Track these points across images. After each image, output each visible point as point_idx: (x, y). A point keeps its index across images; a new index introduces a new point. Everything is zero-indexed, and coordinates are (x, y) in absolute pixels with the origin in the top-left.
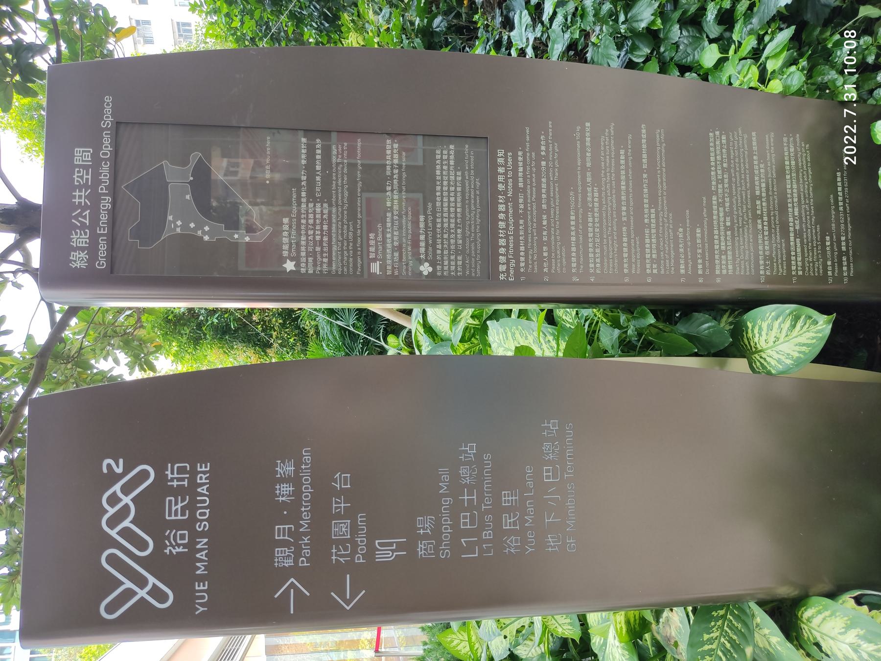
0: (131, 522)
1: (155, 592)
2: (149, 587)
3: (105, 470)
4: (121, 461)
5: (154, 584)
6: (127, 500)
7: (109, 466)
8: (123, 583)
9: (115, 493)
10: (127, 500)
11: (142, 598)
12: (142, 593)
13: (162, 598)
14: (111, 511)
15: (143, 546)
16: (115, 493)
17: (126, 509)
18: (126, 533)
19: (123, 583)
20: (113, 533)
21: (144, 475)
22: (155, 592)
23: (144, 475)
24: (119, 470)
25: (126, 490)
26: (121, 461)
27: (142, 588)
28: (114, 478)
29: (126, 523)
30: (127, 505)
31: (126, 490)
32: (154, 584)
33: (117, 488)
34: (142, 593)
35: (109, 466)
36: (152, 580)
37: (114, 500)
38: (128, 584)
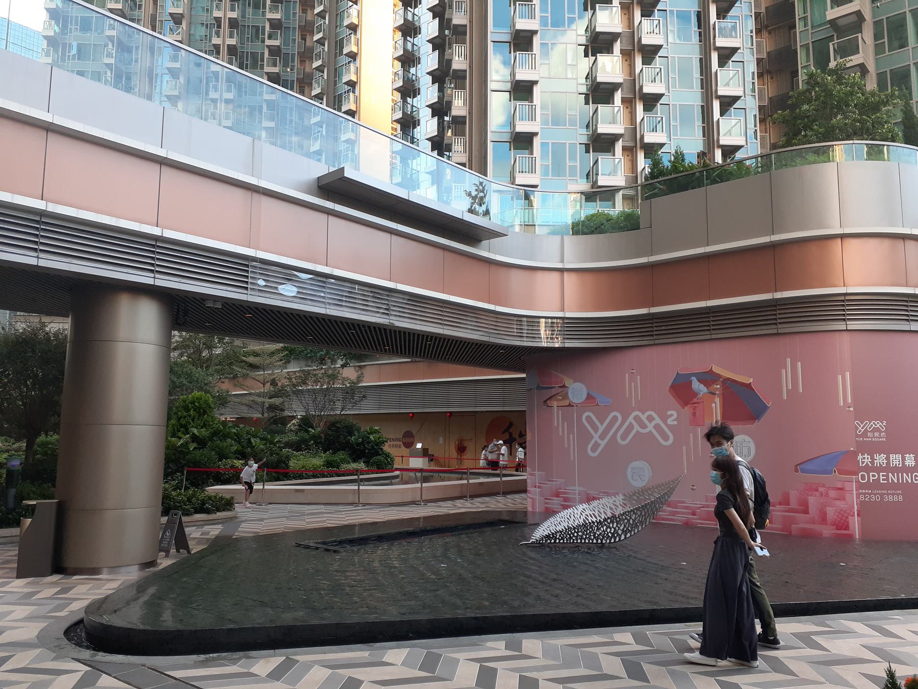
1: (596, 445)
2: (599, 441)
3: (669, 413)
4: (676, 423)
6: (650, 427)
7: (672, 415)
8: (602, 424)
10: (650, 427)
13: (594, 449)
14: (644, 417)
15: (623, 438)
17: (645, 427)
18: (631, 427)
19: (602, 424)
21: (666, 438)
22: (596, 445)
23: (666, 438)
25: (657, 427)
26: (676, 423)
27: (600, 437)
28: (664, 419)
29: (637, 428)
31: (657, 427)
33: (658, 420)
34: (596, 437)
35: (672, 415)
36: (603, 443)
37: (650, 419)
38: (601, 429)
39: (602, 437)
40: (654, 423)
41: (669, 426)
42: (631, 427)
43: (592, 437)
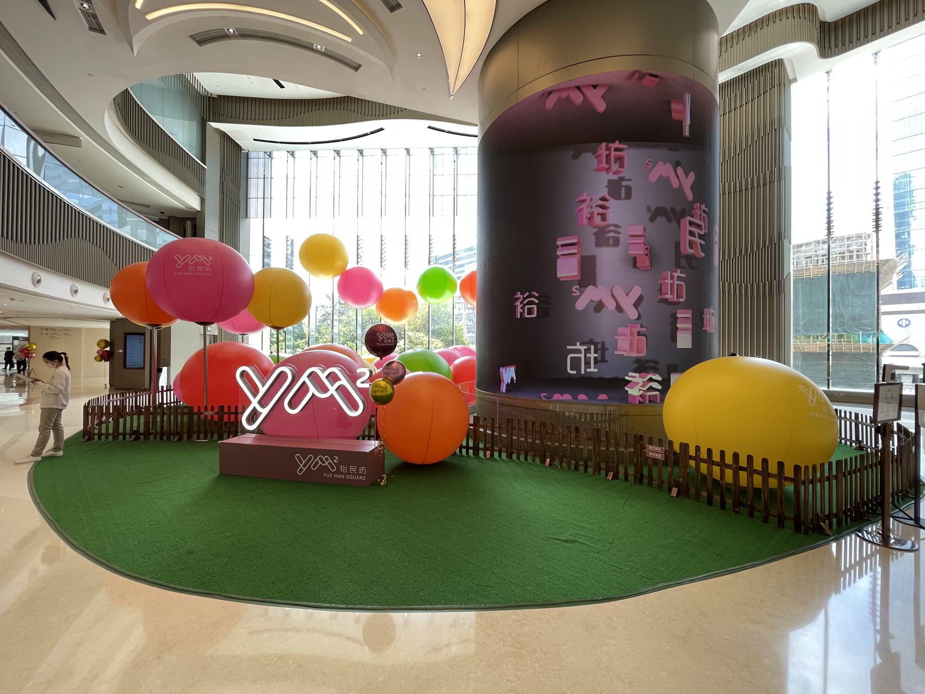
0: (313, 395)
1: (254, 415)
2: (259, 409)
8: (263, 386)
10: (332, 390)
11: (250, 402)
14: (323, 376)
15: (292, 405)
17: (325, 389)
18: (304, 388)
19: (263, 386)
20: (304, 378)
21: (355, 407)
23: (355, 407)
24: (359, 384)
27: (260, 402)
29: (312, 390)
30: (326, 390)
31: (342, 390)
33: (344, 382)
34: (255, 403)
36: (264, 412)
37: (333, 378)
38: (262, 390)
41: (361, 391)
43: (249, 402)
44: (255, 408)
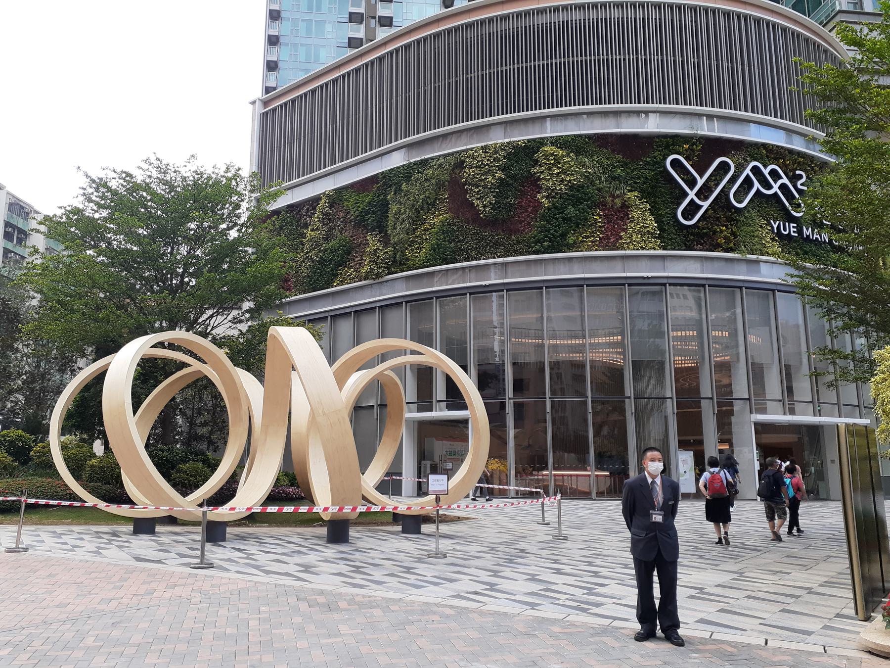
1: (693, 208)
5: (701, 207)
8: (701, 177)
9: (781, 178)
10: (776, 188)
11: (686, 195)
12: (692, 195)
13: (687, 214)
14: (766, 172)
16: (781, 178)
18: (748, 182)
20: (748, 171)
22: (693, 208)
25: (783, 187)
27: (697, 195)
28: (794, 179)
29: (757, 185)
30: (770, 187)
31: (783, 187)
32: (701, 207)
33: (785, 180)
34: (692, 195)
36: (706, 205)
38: (700, 182)
39: (703, 193)
40: (780, 182)
42: (748, 182)
43: (686, 195)
44: (692, 200)
